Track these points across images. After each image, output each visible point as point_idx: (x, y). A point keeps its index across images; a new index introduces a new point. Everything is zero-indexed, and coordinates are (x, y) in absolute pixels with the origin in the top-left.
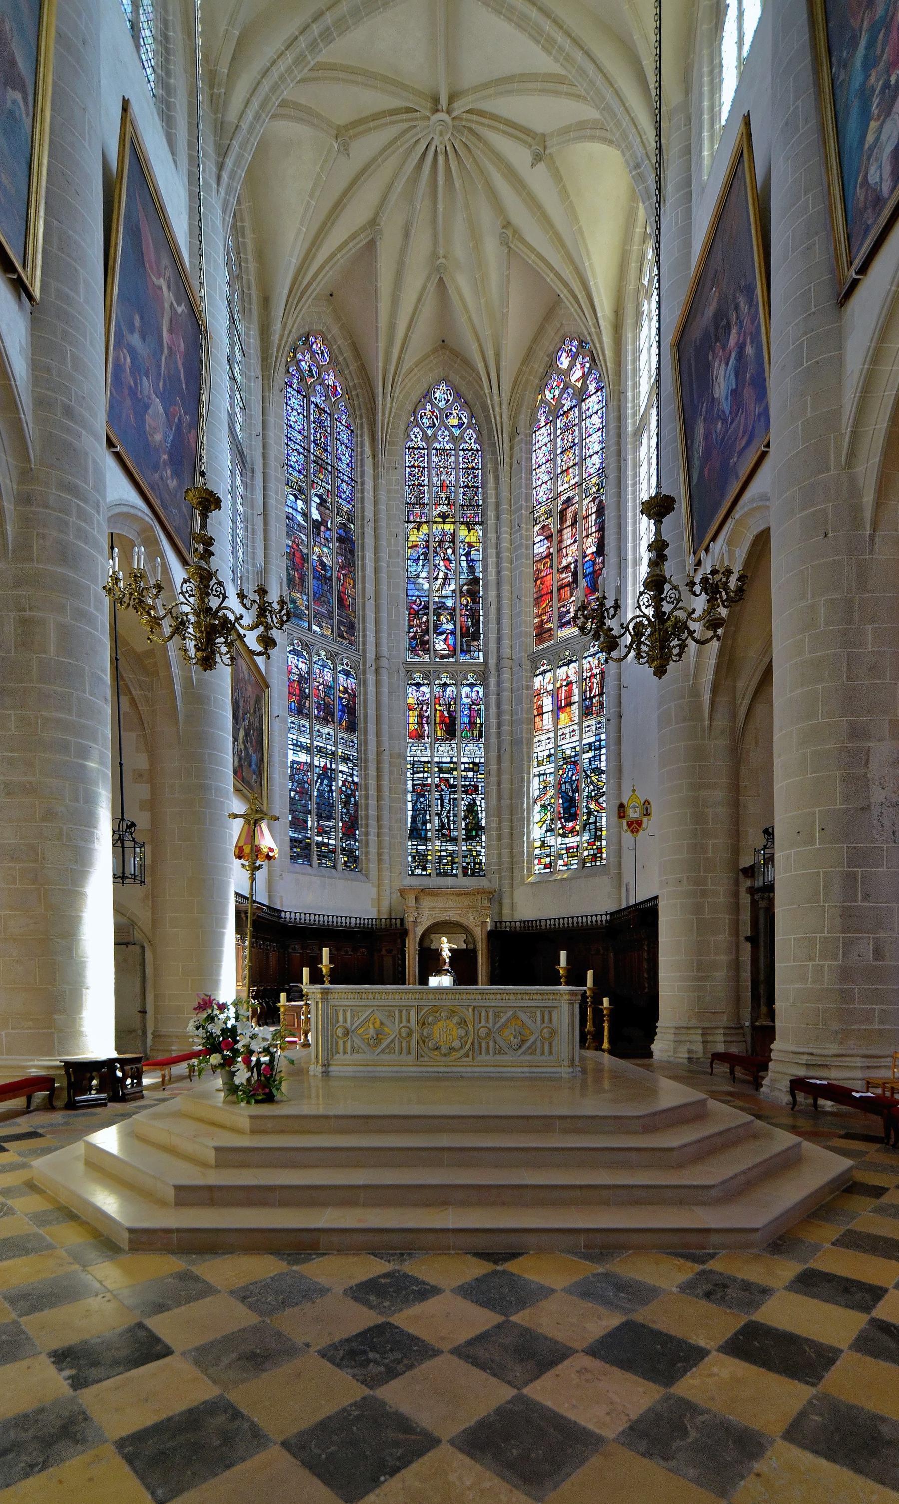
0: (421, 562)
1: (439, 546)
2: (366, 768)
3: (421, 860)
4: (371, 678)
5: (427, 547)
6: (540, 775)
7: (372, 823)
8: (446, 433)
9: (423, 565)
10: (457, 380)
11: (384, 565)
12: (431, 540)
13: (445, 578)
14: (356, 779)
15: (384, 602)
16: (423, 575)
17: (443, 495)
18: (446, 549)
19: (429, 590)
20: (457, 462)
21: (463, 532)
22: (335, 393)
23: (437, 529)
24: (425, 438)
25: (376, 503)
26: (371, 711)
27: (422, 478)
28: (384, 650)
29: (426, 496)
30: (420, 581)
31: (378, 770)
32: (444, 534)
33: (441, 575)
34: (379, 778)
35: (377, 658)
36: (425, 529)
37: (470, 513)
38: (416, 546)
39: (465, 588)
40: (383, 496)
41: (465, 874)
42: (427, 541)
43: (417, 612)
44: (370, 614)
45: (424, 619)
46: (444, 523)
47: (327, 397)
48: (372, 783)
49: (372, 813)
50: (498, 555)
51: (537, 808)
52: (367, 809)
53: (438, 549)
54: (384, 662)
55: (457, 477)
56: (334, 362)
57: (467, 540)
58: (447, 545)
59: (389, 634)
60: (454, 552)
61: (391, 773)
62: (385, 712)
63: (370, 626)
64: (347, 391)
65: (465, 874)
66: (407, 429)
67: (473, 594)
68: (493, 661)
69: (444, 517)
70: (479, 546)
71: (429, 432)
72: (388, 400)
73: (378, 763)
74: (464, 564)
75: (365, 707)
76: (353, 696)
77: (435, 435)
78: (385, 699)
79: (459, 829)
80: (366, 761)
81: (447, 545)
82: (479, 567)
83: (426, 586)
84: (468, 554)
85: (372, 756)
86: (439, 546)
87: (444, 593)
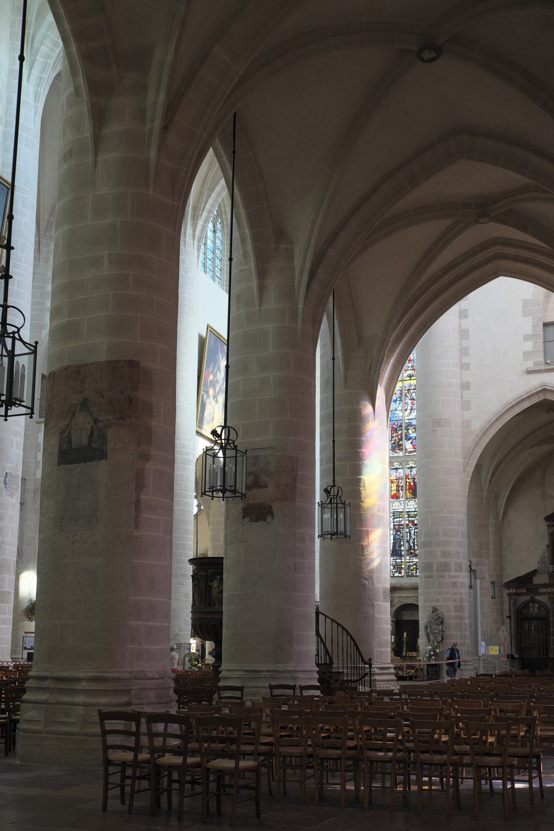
0: (398, 402)
1: (408, 392)
5: (401, 394)
9: (399, 404)
12: (403, 389)
13: (411, 409)
16: (400, 408)
18: (412, 394)
23: (407, 383)
30: (397, 412)
32: (411, 385)
33: (409, 408)
42: (401, 391)
46: (410, 380)
53: (407, 394)
58: (412, 391)
69: (410, 376)
81: (412, 391)
83: (401, 414)
86: (408, 392)
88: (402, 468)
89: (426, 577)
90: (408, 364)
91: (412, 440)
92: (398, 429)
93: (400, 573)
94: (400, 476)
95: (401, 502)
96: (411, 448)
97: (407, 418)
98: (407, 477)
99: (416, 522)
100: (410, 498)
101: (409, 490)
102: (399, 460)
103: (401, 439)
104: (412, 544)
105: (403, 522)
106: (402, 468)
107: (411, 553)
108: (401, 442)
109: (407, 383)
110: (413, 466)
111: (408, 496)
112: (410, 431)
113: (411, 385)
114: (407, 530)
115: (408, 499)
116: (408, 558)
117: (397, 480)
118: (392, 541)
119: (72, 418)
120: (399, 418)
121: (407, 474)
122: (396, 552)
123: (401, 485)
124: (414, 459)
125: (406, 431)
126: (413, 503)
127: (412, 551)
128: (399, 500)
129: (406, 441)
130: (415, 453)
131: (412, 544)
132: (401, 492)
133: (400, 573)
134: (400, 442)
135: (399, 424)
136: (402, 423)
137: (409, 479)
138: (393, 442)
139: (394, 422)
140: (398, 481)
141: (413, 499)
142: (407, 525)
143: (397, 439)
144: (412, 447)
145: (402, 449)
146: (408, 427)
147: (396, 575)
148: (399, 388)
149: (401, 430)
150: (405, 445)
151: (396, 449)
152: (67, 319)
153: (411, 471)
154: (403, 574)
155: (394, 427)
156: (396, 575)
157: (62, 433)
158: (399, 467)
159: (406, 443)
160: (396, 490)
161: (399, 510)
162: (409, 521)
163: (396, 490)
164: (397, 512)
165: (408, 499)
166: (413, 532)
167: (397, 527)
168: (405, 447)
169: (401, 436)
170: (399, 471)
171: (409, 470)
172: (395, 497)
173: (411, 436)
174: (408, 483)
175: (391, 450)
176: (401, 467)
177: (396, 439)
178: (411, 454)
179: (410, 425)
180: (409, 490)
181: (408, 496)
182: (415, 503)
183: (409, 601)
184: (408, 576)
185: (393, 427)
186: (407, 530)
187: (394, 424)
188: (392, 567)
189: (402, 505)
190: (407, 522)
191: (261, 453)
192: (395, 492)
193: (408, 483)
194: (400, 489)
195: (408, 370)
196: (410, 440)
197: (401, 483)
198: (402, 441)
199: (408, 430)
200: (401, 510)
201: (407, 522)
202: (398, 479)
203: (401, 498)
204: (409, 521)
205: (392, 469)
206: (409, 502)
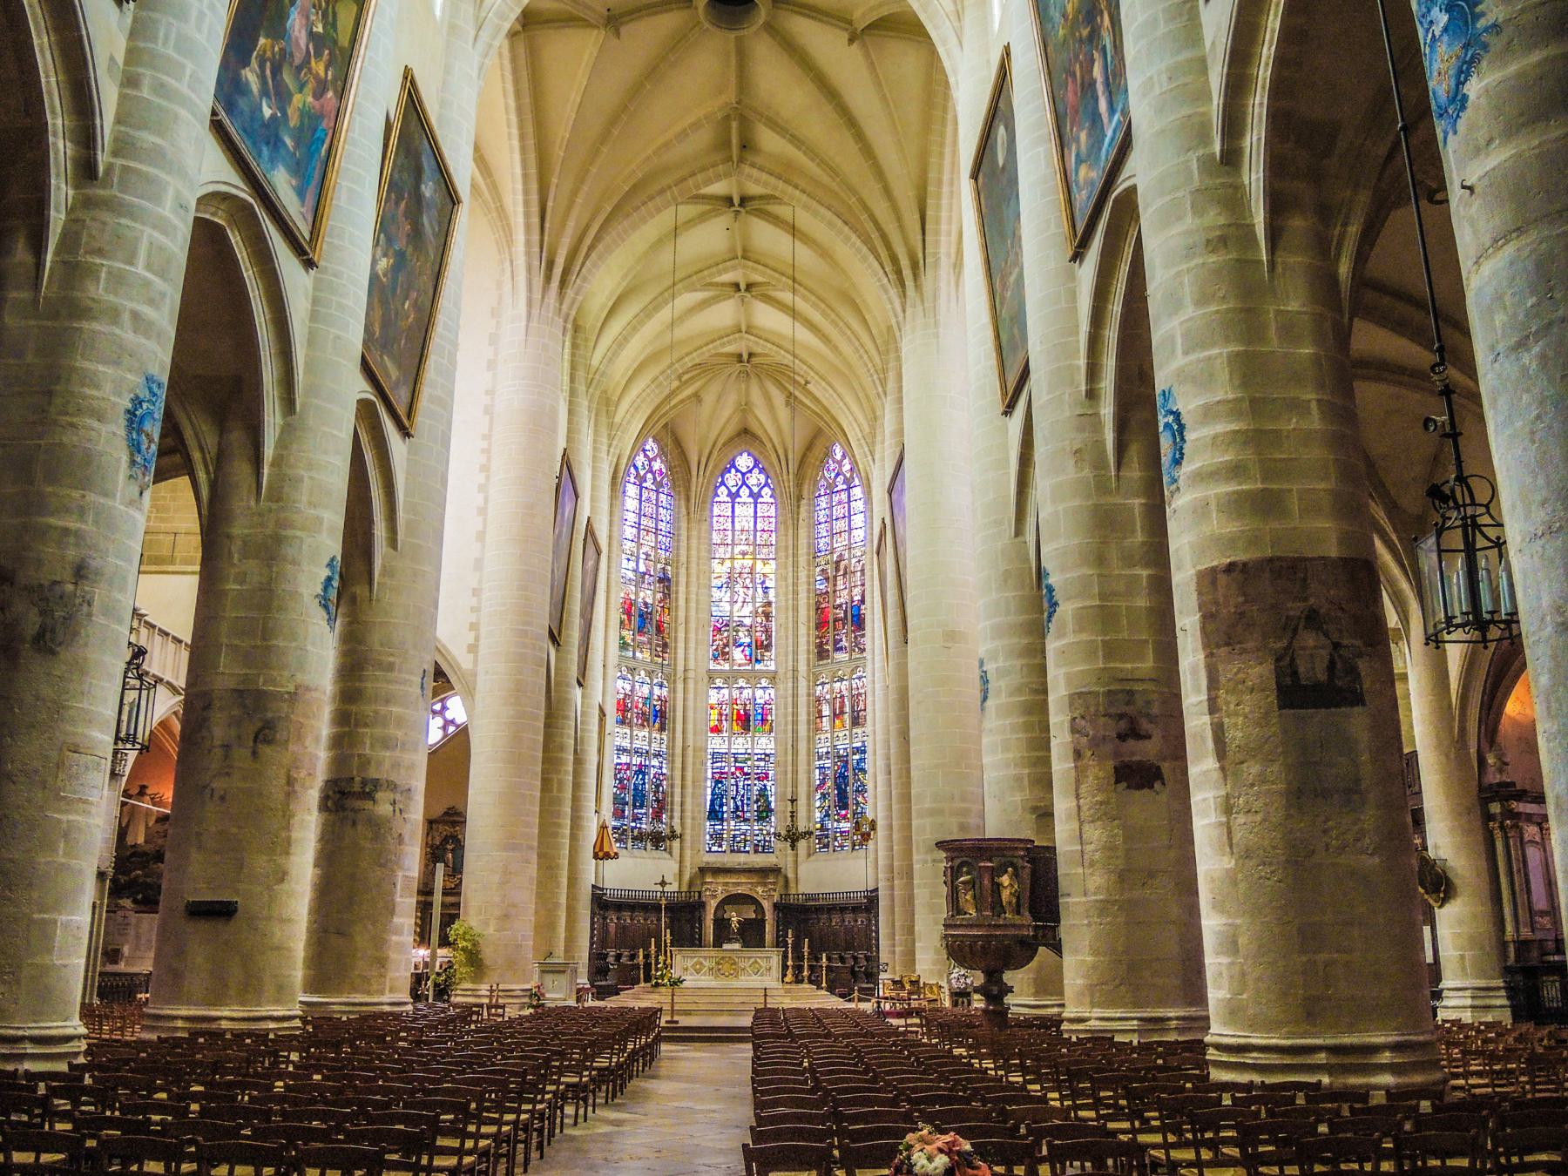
2: (673, 762)
3: (717, 837)
4: (680, 686)
6: (820, 768)
7: (677, 808)
8: (747, 491)
10: (756, 454)
11: (693, 596)
14: (664, 771)
15: (692, 625)
17: (744, 537)
19: (731, 612)
20: (756, 512)
21: (759, 564)
22: (661, 473)
24: (730, 494)
25: (688, 549)
26: (679, 714)
28: (692, 665)
29: (730, 538)
31: (683, 763)
32: (743, 567)
33: (741, 599)
34: (683, 769)
35: (685, 670)
36: (728, 563)
37: (765, 550)
39: (760, 610)
40: (694, 542)
41: (756, 851)
43: (720, 630)
44: (681, 635)
47: (655, 479)
48: (678, 773)
49: (677, 799)
50: (787, 586)
51: (818, 796)
52: (672, 796)
54: (691, 674)
55: (755, 523)
56: (663, 452)
59: (696, 649)
61: (694, 763)
62: (690, 714)
63: (681, 645)
64: (670, 468)
65: (756, 851)
66: (717, 488)
67: (767, 616)
68: (781, 671)
69: (744, 554)
70: (772, 576)
71: (734, 490)
72: (701, 479)
73: (683, 756)
74: (760, 591)
75: (674, 711)
76: (664, 701)
77: (738, 490)
78: (690, 703)
79: (751, 811)
80: (673, 755)
82: (772, 593)
84: (763, 583)
85: (678, 750)
89: (934, 861)
93: (720, 846)
99: (746, 770)
102: (723, 675)
103: (726, 645)
104: (739, 803)
105: (726, 769)
107: (738, 817)
109: (738, 564)
112: (741, 634)
113: (743, 567)
114: (733, 781)
116: (733, 823)
118: (709, 798)
119: (1292, 638)
122: (715, 814)
127: (740, 814)
131: (739, 803)
133: (720, 846)
142: (733, 774)
147: (715, 848)
152: (1260, 486)
154: (724, 848)
156: (715, 848)
157: (1277, 660)
162: (737, 768)
166: (741, 784)
167: (717, 776)
170: (722, 691)
171: (738, 692)
172: (716, 730)
179: (741, 624)
183: (740, 890)
184: (732, 851)
186: (733, 781)
188: (708, 837)
190: (733, 769)
191: (1137, 687)
199: (737, 631)
201: (733, 769)
204: (737, 768)
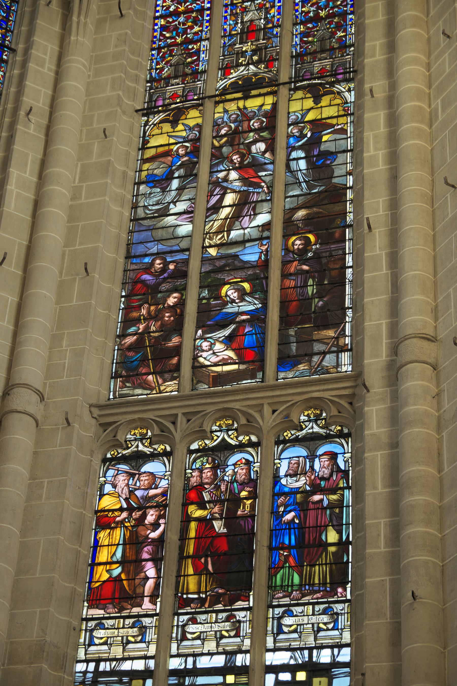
0: (175, 184)
16: (181, 207)
27: (196, 29)
30: (170, 220)
38: (167, 154)
45: (171, 301)
57: (310, 117)
60: (271, 148)
86: (230, 143)
87: (234, 234)
88: (166, 454)
90: (238, 46)
91: (233, 327)
92: (164, 287)
94: (152, 492)
95: (146, 621)
96: (225, 362)
97: (217, 240)
98: (193, 495)
100: (202, 601)
101: (195, 557)
106: (166, 454)
108: (175, 340)
110: (233, 442)
111: (192, 586)
115: (187, 603)
117: (130, 509)
120: (173, 242)
121: (194, 481)
123: (154, 535)
124: (237, 405)
125: (205, 293)
126: (216, 627)
128: (136, 610)
129: (200, 332)
130: (246, 383)
132: (151, 572)
134: (168, 338)
135: (172, 267)
136: (186, 262)
137: (202, 505)
138: (130, 340)
139: (147, 260)
140: (136, 515)
141: (220, 607)
143: (153, 328)
144: (231, 354)
145: (177, 368)
146: (220, 276)
148: (184, 134)
149: (182, 290)
150: (195, 348)
151: (144, 370)
153: (214, 468)
155: (143, 282)
158: (147, 450)
159: (198, 342)
160: (122, 562)
161: (126, 666)
163: (122, 562)
164: (112, 673)
165: (187, 603)
168: (195, 358)
169: (174, 314)
173: (230, 309)
174: (193, 525)
175: (116, 376)
176: (160, 448)
177: (147, 328)
178: (228, 387)
180: (195, 557)
181: (192, 586)
182: (227, 625)
185: (137, 282)
187: (148, 269)
189: (151, 635)
192: (117, 571)
193: (193, 525)
194: (145, 556)
195: (239, 65)
196: (224, 326)
197: (155, 526)
198: (181, 335)
200: (139, 665)
202: (139, 509)
203: (146, 600)
205: (111, 460)
206: (194, 621)
